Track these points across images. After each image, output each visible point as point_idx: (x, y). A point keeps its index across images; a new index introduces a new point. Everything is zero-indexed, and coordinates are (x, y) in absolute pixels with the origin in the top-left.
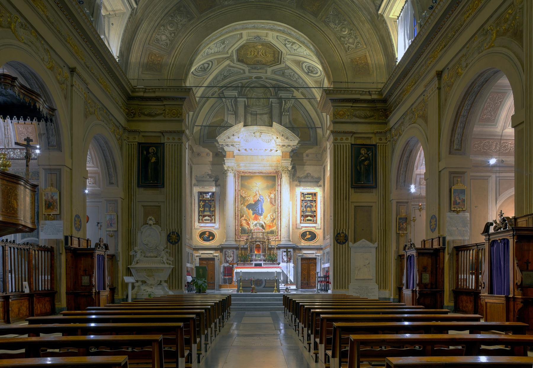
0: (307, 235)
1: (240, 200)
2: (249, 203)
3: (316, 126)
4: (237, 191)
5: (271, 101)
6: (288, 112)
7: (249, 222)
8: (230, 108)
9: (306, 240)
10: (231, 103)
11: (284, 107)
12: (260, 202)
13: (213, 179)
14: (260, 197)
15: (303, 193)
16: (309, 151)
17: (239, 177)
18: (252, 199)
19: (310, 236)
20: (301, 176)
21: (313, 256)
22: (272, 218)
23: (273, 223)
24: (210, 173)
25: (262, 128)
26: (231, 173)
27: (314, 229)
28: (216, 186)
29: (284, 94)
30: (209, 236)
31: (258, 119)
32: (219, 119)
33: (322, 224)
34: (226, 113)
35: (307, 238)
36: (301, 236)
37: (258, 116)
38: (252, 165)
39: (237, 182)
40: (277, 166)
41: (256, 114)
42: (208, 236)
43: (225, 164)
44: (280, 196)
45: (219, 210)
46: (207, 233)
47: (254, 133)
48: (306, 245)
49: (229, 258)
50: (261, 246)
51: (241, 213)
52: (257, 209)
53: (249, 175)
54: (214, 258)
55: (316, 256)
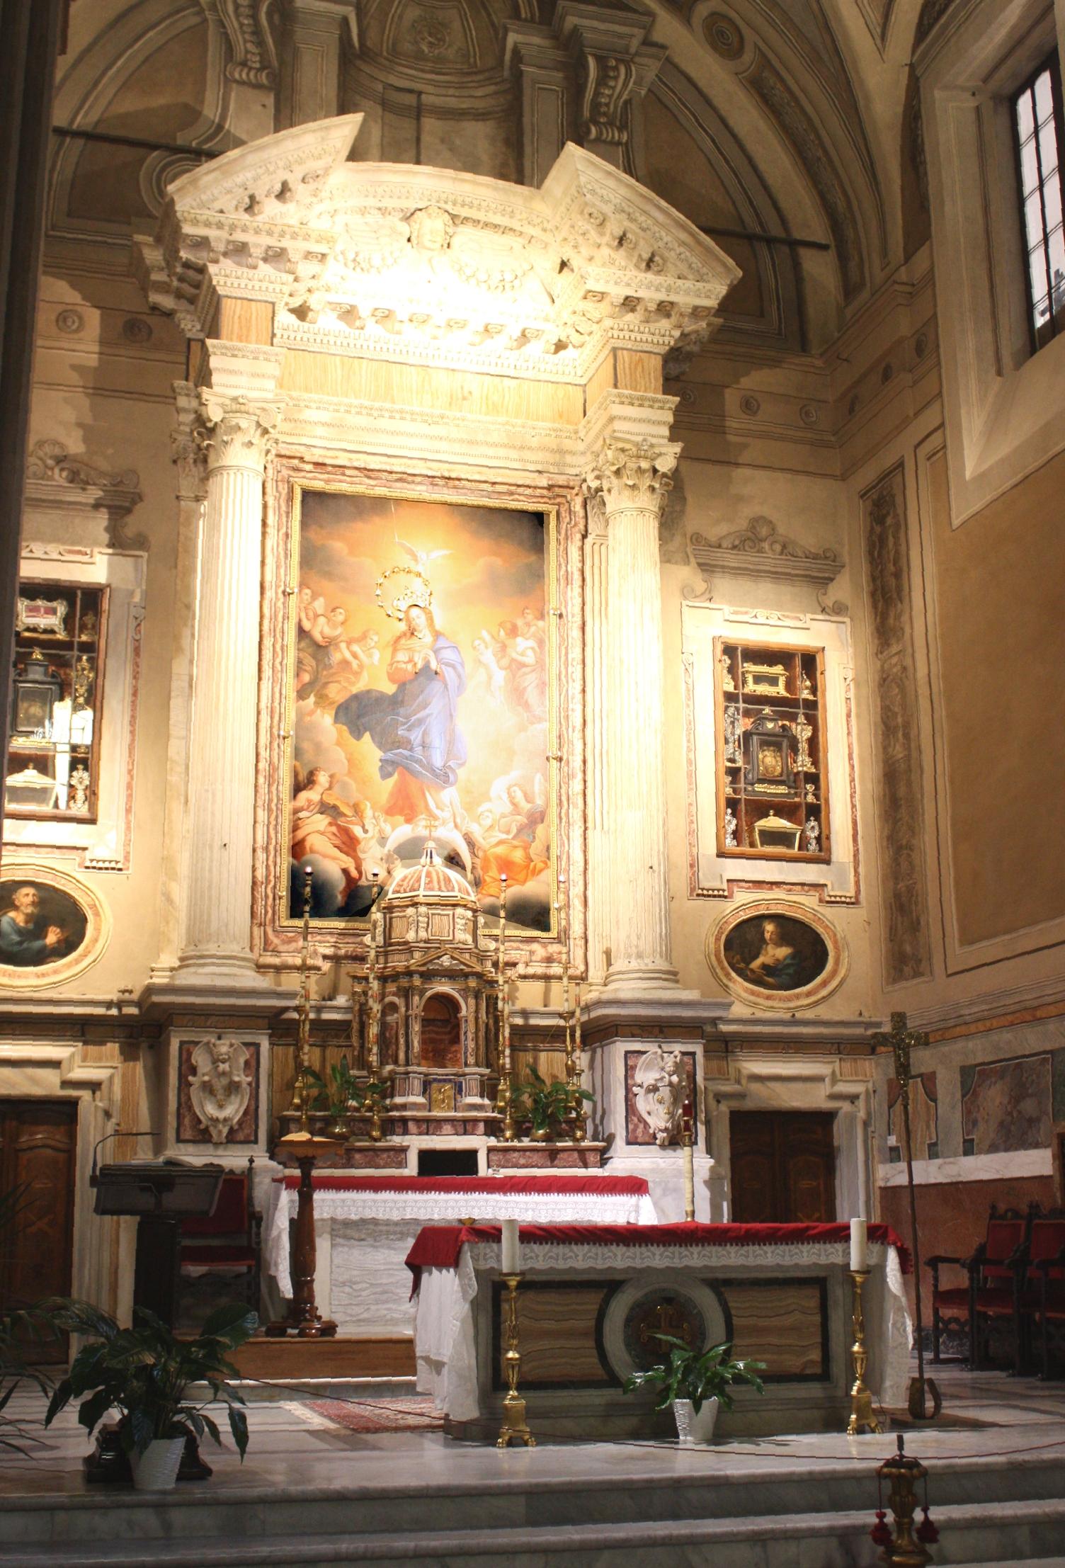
0: (763, 940)
1: (291, 660)
2: (358, 687)
3: (797, 235)
4: (269, 594)
5: (516, 51)
6: (620, 130)
7: (357, 831)
8: (243, 45)
9: (758, 982)
10: (255, 17)
11: (597, 94)
12: (436, 686)
13: (94, 494)
14: (436, 652)
15: (729, 650)
16: (757, 380)
17: (290, 499)
18: (376, 655)
19: (783, 952)
20: (714, 532)
21: (815, 1098)
22: (526, 806)
23: (526, 848)
24: (75, 445)
25: (467, 188)
26: (254, 450)
27: (809, 901)
28: (118, 543)
29: (596, 24)
30: (38, 925)
31: (426, 138)
32: (161, 101)
33: (861, 870)
34: (211, 75)
35: (764, 967)
36: (729, 945)
37: (429, 123)
38: (384, 423)
39: (271, 530)
40: (561, 452)
41: (418, 112)
42: (29, 917)
43: (204, 377)
44: (575, 653)
45: (127, 728)
46: (25, 897)
47: (408, 217)
48: (760, 1014)
49: (221, 1107)
50: (466, 1009)
51: (298, 753)
52: (415, 736)
53: (360, 489)
54: (73, 1104)
55: (833, 1097)
